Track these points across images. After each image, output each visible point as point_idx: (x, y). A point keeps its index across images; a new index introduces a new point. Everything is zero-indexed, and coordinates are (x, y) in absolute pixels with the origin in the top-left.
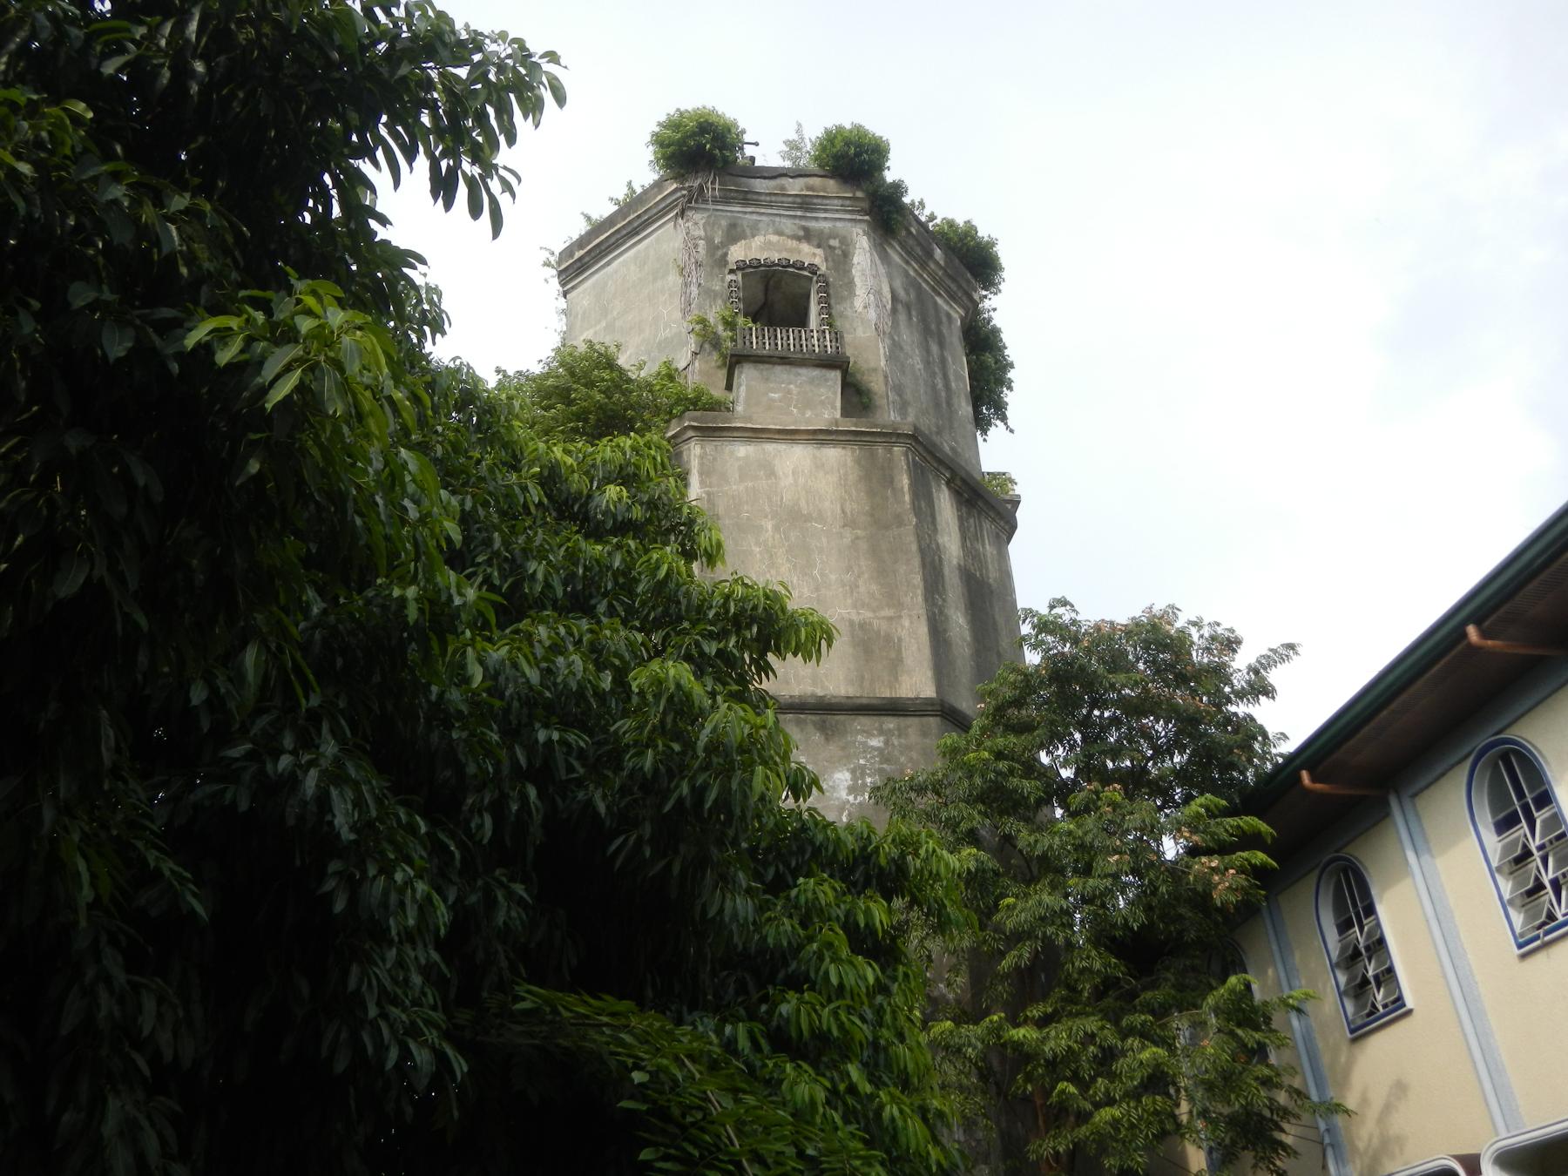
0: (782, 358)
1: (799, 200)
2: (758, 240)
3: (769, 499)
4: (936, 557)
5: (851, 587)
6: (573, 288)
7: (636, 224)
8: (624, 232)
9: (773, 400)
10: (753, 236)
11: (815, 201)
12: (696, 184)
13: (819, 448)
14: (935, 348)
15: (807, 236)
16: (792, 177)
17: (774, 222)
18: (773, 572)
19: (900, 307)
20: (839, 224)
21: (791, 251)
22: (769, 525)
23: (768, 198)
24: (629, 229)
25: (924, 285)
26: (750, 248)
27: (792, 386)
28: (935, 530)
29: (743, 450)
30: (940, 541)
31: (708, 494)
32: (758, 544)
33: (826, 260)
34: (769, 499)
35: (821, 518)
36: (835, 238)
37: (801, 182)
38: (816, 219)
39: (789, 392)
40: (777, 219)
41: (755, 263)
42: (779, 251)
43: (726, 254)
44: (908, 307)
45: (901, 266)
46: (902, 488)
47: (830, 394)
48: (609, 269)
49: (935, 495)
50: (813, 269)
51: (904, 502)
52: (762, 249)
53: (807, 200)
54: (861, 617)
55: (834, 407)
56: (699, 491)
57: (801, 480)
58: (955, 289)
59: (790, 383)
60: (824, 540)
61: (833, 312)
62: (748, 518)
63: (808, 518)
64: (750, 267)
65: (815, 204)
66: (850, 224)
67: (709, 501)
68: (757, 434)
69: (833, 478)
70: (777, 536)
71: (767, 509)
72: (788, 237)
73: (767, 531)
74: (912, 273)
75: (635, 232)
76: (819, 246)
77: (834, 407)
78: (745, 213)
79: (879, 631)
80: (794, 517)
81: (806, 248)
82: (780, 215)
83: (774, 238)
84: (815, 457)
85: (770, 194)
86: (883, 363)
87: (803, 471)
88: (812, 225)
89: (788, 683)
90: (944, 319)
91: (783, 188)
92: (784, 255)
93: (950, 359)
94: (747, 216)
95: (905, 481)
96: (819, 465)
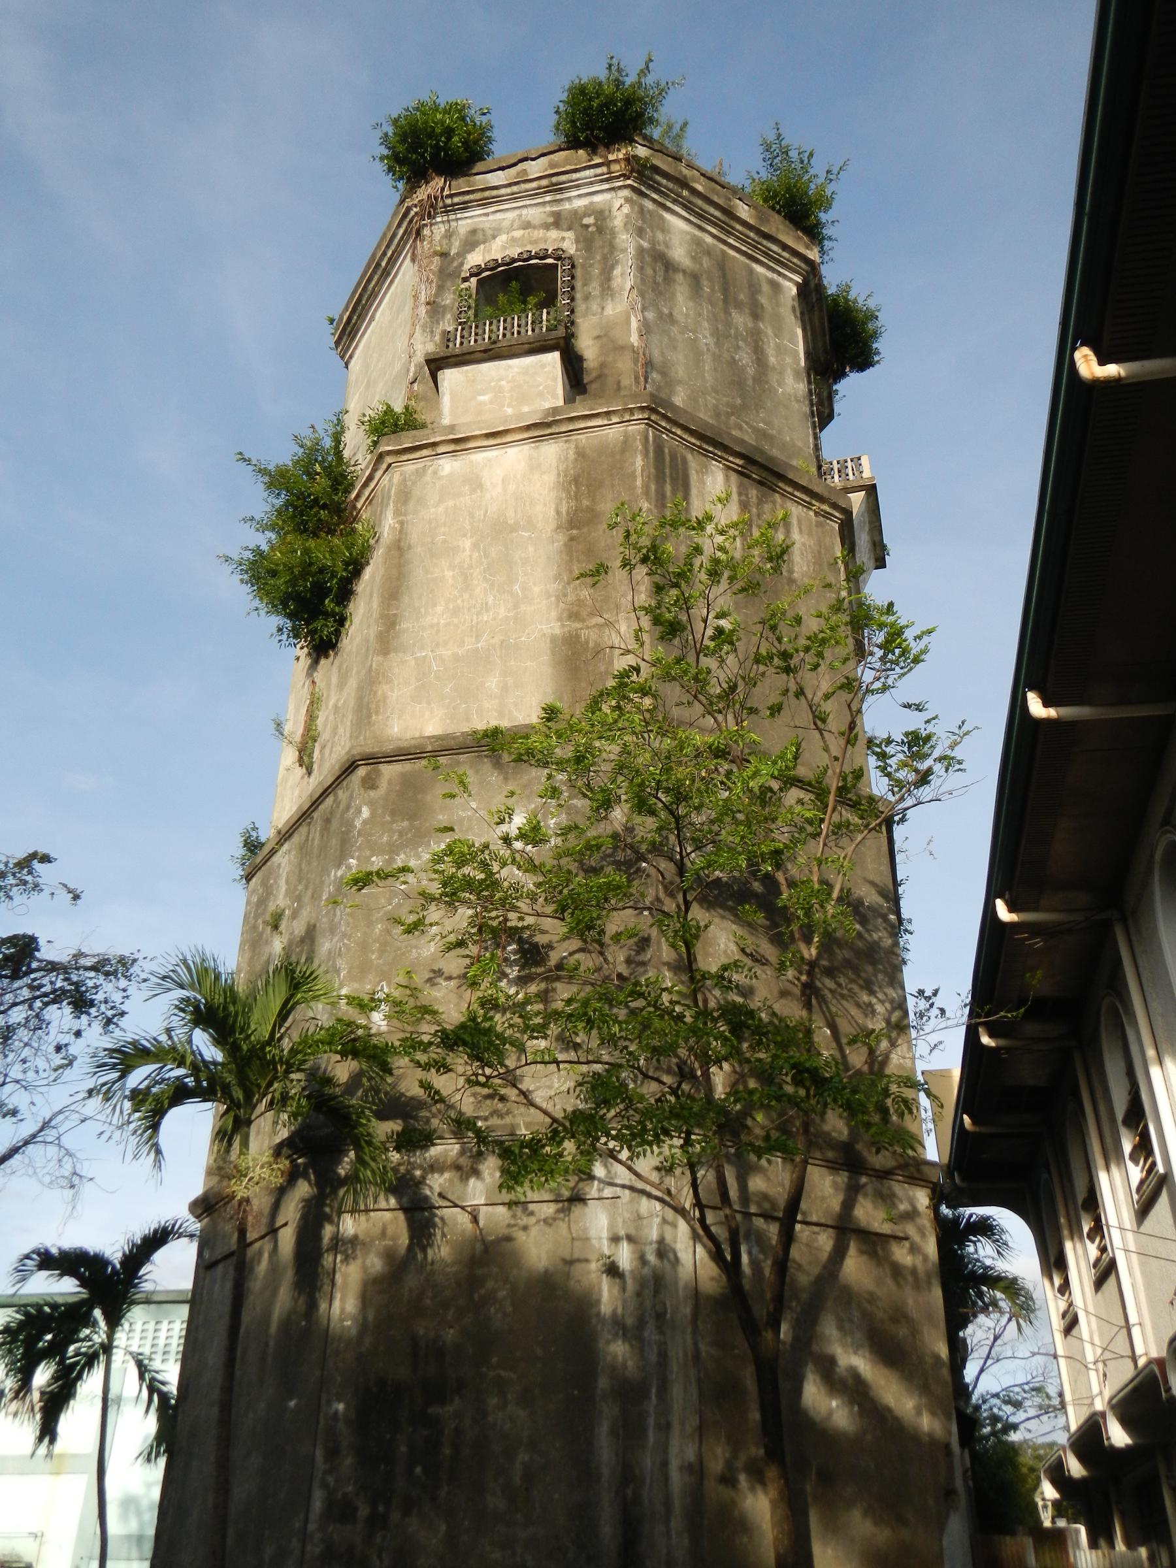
0: (485, 351)
1: (544, 182)
2: (502, 238)
3: (471, 515)
5: (557, 597)
6: (351, 357)
7: (384, 264)
8: (376, 277)
9: (481, 404)
10: (494, 237)
12: (425, 197)
13: (537, 447)
14: (741, 320)
15: (557, 221)
16: (533, 159)
17: (520, 216)
18: (466, 596)
19: (680, 277)
20: (597, 198)
21: (536, 242)
22: (467, 544)
23: (509, 190)
24: (379, 272)
25: (732, 252)
26: (489, 251)
27: (503, 383)
29: (448, 466)
31: (402, 523)
33: (577, 241)
34: (471, 515)
35: (530, 525)
36: (589, 216)
38: (569, 199)
39: (500, 390)
40: (524, 211)
41: (492, 265)
43: (462, 264)
44: (695, 279)
45: (688, 233)
46: (635, 471)
47: (549, 382)
48: (373, 324)
49: (693, 477)
50: (559, 256)
51: (635, 488)
52: (504, 248)
54: (566, 629)
55: (555, 396)
56: (391, 522)
57: (511, 488)
58: (780, 251)
59: (501, 379)
60: (531, 549)
61: (578, 296)
62: (444, 541)
63: (514, 528)
64: (488, 270)
65: (564, 183)
66: (607, 196)
67: (401, 531)
69: (550, 478)
70: (476, 555)
71: (468, 527)
72: (534, 227)
73: (464, 550)
74: (709, 240)
75: (386, 273)
76: (569, 229)
78: (487, 215)
79: (587, 642)
81: (554, 234)
82: (525, 206)
83: (518, 234)
84: (531, 458)
85: (510, 185)
86: (634, 339)
87: (515, 477)
88: (567, 206)
89: (468, 720)
90: (765, 288)
91: (525, 172)
93: (770, 331)
94: (491, 217)
95: (639, 462)
96: (534, 466)
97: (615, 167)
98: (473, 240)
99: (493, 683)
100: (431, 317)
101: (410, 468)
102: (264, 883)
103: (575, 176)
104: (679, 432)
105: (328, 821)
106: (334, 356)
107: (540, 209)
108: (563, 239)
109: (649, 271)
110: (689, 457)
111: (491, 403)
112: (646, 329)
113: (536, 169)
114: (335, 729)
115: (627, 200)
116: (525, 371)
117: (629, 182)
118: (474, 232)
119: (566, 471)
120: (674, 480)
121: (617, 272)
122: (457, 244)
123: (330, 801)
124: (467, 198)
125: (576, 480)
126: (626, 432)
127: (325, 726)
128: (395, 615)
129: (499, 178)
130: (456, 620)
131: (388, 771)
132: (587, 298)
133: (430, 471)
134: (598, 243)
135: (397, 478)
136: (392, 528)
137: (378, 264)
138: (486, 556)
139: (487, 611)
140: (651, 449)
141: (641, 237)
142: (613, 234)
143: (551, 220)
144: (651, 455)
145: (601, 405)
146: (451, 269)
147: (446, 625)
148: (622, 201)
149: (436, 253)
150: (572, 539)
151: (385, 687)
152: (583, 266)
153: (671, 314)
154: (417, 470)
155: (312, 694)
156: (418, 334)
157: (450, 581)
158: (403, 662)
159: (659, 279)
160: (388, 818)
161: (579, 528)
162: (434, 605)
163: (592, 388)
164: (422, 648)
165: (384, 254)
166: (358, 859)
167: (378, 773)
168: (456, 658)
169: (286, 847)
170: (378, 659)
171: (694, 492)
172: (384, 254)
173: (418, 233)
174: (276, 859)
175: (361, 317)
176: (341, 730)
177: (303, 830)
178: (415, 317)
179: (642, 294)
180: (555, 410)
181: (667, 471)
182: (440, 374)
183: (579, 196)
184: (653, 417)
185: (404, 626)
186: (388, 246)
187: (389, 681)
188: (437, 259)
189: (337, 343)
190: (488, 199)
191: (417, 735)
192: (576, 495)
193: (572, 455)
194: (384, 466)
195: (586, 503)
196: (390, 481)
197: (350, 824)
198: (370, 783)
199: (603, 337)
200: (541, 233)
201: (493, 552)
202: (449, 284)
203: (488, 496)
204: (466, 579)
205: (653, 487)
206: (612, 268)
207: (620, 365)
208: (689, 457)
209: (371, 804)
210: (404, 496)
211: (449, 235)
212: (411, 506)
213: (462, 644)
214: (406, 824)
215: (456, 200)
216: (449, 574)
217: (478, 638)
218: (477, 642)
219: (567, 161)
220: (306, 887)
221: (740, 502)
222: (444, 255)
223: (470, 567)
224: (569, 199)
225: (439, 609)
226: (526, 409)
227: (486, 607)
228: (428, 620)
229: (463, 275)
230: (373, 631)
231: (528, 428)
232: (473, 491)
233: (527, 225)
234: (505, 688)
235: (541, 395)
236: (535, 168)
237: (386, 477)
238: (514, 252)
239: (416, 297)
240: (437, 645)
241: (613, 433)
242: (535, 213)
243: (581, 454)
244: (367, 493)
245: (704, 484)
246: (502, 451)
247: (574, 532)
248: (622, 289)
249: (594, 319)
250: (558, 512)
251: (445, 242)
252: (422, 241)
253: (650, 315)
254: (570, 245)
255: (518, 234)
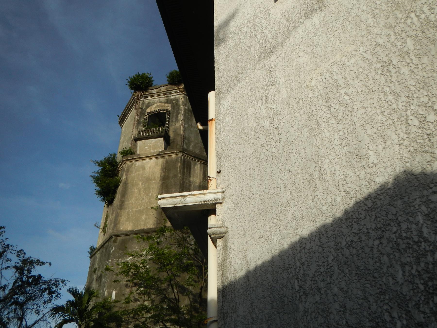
1: (165, 92)
2: (155, 105)
3: (142, 176)
4: (188, 185)
6: (123, 126)
9: (146, 149)
10: (153, 105)
11: (169, 92)
15: (167, 102)
18: (139, 196)
20: (177, 96)
21: (162, 107)
22: (140, 183)
23: (157, 94)
26: (152, 108)
28: (190, 176)
29: (138, 163)
30: (191, 179)
31: (127, 177)
32: (137, 189)
33: (171, 107)
35: (154, 179)
36: (174, 100)
37: (165, 87)
39: (150, 146)
40: (160, 99)
42: (159, 107)
43: (146, 111)
50: (167, 110)
51: (178, 171)
52: (155, 108)
53: (167, 92)
55: (162, 148)
57: (151, 169)
60: (154, 185)
61: (170, 121)
63: (151, 180)
66: (179, 96)
68: (141, 159)
69: (160, 167)
70: (142, 186)
71: (141, 179)
75: (130, 110)
76: (170, 104)
77: (162, 148)
80: (148, 180)
81: (166, 105)
83: (158, 104)
84: (156, 162)
86: (182, 133)
88: (170, 98)
89: (137, 226)
91: (160, 90)
92: (161, 108)
94: (153, 100)
95: (179, 164)
96: (157, 164)
97: (181, 90)
98: (149, 105)
99: (143, 218)
100: (138, 125)
101: (129, 163)
102: (94, 260)
103: (172, 91)
104: (189, 156)
105: (106, 249)
106: (119, 125)
107: (164, 98)
108: (168, 106)
109: (187, 115)
110: (192, 162)
111: (148, 149)
112: (185, 129)
113: (163, 89)
114: (110, 225)
115: (183, 97)
116: (156, 142)
117: (184, 93)
118: (149, 103)
119: (163, 166)
120: (187, 168)
121: (179, 115)
122: (145, 106)
123: (107, 244)
124: (147, 95)
125: (165, 168)
126: (177, 157)
127: (108, 223)
128: (124, 200)
129: (155, 91)
130: (136, 202)
131: (119, 239)
132: (172, 121)
133: (134, 165)
134: (176, 108)
135: (126, 166)
136: (125, 179)
137: (128, 108)
138: (144, 186)
139: (144, 200)
140: (182, 161)
141: (186, 106)
142: (179, 106)
143: (166, 101)
144: (182, 162)
145: (172, 151)
146: (143, 112)
147: (134, 203)
148: (182, 97)
149: (140, 108)
150: (163, 183)
151: (120, 218)
152: (172, 113)
153: (191, 124)
154: (131, 164)
155: (107, 214)
156: (134, 129)
157: (136, 192)
158: (124, 212)
159: (189, 116)
160: (118, 250)
161: (165, 180)
162: (132, 198)
163: (172, 144)
164: (129, 209)
165: (129, 106)
166: (111, 260)
167: (117, 239)
168: (136, 211)
169: (98, 252)
170: (119, 211)
171: (192, 170)
172: (129, 106)
173: (137, 102)
174: (96, 255)
175: (125, 118)
176: (111, 226)
177: (102, 249)
178: (134, 124)
179: (184, 121)
180: (162, 152)
181: (186, 166)
182: (137, 142)
183: (173, 96)
184: (183, 154)
185: (125, 203)
186: (130, 104)
187: (121, 216)
188: (140, 110)
189: (119, 123)
190: (152, 95)
191: (126, 230)
192: (165, 172)
193: (165, 162)
194: (124, 163)
195: (167, 174)
196: (125, 166)
197: (110, 251)
198: (115, 241)
199: (175, 132)
200: (163, 104)
201: (146, 185)
202: (142, 116)
203: (146, 171)
204: (139, 192)
205: (182, 170)
206: (178, 114)
207: (178, 139)
208: (192, 162)
209: (115, 247)
210: (128, 171)
211: (143, 103)
212: (129, 173)
213: (137, 208)
214: (122, 252)
215: (145, 96)
216: (136, 190)
217: (141, 206)
218: (141, 207)
219: (170, 88)
220: (101, 264)
221: (203, 171)
222: (142, 109)
223: (141, 189)
224: (170, 96)
225: (133, 199)
226: (156, 151)
227: (143, 199)
228: (131, 202)
229: (145, 114)
230: (119, 203)
231: (155, 155)
232: (143, 170)
233: (161, 102)
234: (146, 219)
235: (159, 147)
236: (163, 89)
237: (124, 165)
238: (157, 109)
239: (135, 119)
240: (132, 208)
241: (174, 157)
242: (163, 99)
243: (167, 162)
244: (120, 168)
245: (195, 168)
246: (150, 160)
247: (164, 181)
248: (180, 120)
249: (173, 127)
250: (161, 176)
251: (142, 105)
252: (137, 104)
253: (186, 126)
254: (169, 108)
255: (158, 104)
